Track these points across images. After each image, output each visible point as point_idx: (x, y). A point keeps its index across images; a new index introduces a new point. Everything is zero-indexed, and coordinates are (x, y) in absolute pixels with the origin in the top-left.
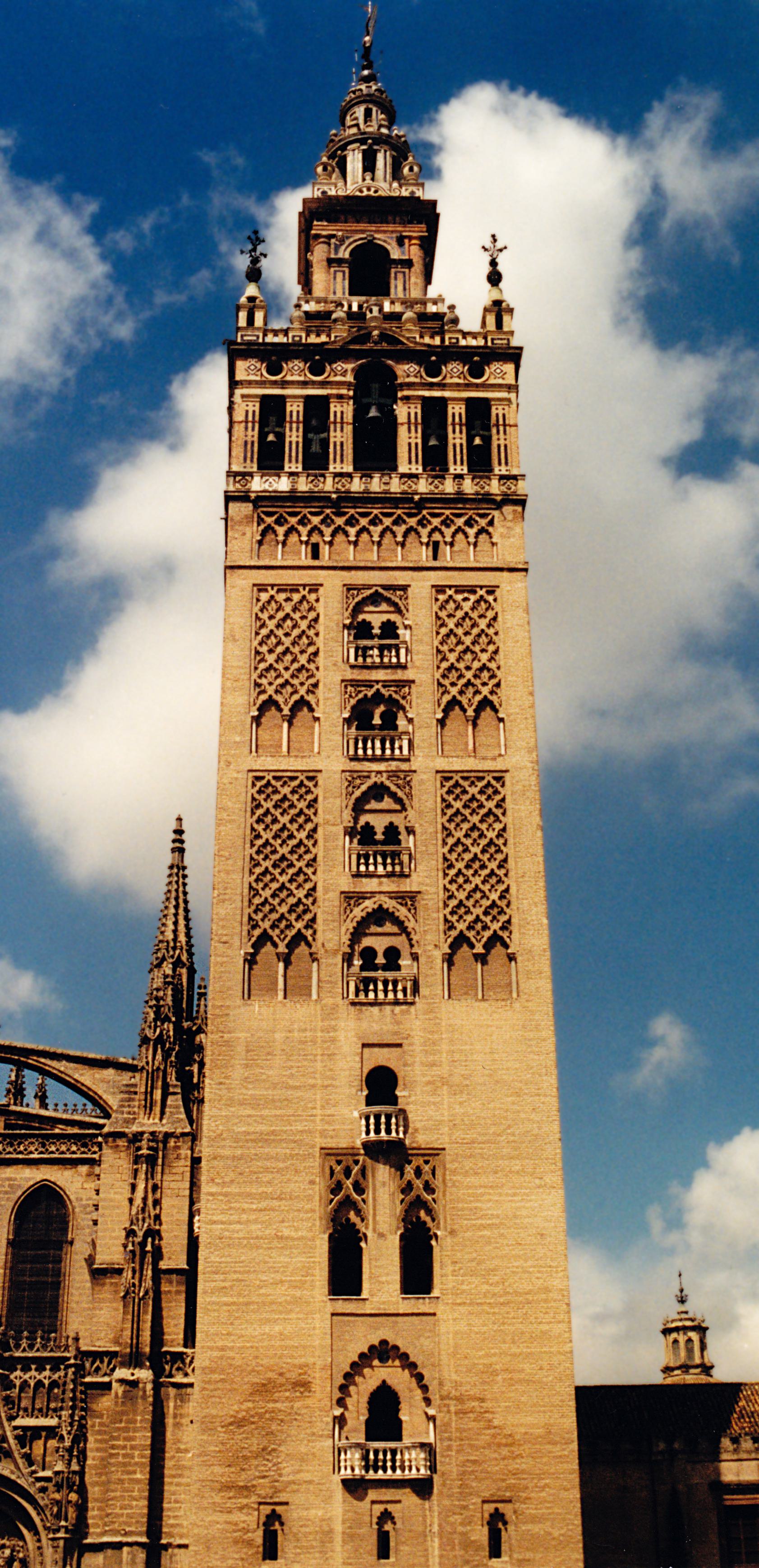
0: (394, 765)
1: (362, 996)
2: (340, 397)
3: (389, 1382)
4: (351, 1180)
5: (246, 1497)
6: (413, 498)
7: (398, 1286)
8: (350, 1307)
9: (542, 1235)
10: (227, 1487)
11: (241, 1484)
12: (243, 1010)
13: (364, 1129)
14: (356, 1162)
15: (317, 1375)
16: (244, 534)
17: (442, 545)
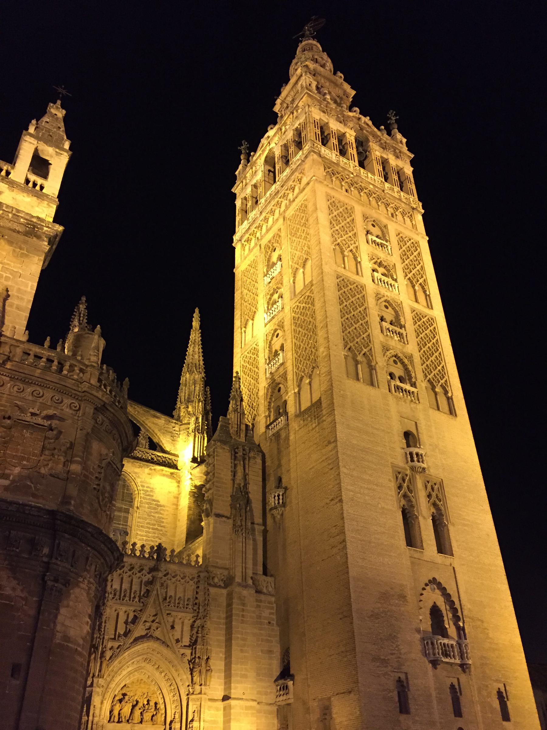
0: (393, 296)
1: (398, 393)
2: (351, 135)
3: (438, 604)
4: (405, 485)
5: (385, 667)
6: (383, 191)
7: (435, 548)
8: (416, 555)
9: (488, 535)
10: (375, 659)
11: (382, 657)
12: (347, 381)
13: (409, 459)
14: (407, 475)
15: (409, 593)
16: (319, 169)
17: (394, 214)
